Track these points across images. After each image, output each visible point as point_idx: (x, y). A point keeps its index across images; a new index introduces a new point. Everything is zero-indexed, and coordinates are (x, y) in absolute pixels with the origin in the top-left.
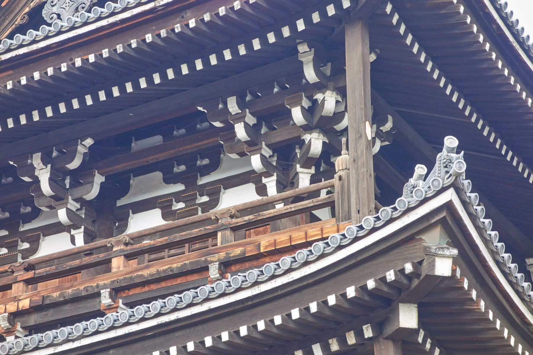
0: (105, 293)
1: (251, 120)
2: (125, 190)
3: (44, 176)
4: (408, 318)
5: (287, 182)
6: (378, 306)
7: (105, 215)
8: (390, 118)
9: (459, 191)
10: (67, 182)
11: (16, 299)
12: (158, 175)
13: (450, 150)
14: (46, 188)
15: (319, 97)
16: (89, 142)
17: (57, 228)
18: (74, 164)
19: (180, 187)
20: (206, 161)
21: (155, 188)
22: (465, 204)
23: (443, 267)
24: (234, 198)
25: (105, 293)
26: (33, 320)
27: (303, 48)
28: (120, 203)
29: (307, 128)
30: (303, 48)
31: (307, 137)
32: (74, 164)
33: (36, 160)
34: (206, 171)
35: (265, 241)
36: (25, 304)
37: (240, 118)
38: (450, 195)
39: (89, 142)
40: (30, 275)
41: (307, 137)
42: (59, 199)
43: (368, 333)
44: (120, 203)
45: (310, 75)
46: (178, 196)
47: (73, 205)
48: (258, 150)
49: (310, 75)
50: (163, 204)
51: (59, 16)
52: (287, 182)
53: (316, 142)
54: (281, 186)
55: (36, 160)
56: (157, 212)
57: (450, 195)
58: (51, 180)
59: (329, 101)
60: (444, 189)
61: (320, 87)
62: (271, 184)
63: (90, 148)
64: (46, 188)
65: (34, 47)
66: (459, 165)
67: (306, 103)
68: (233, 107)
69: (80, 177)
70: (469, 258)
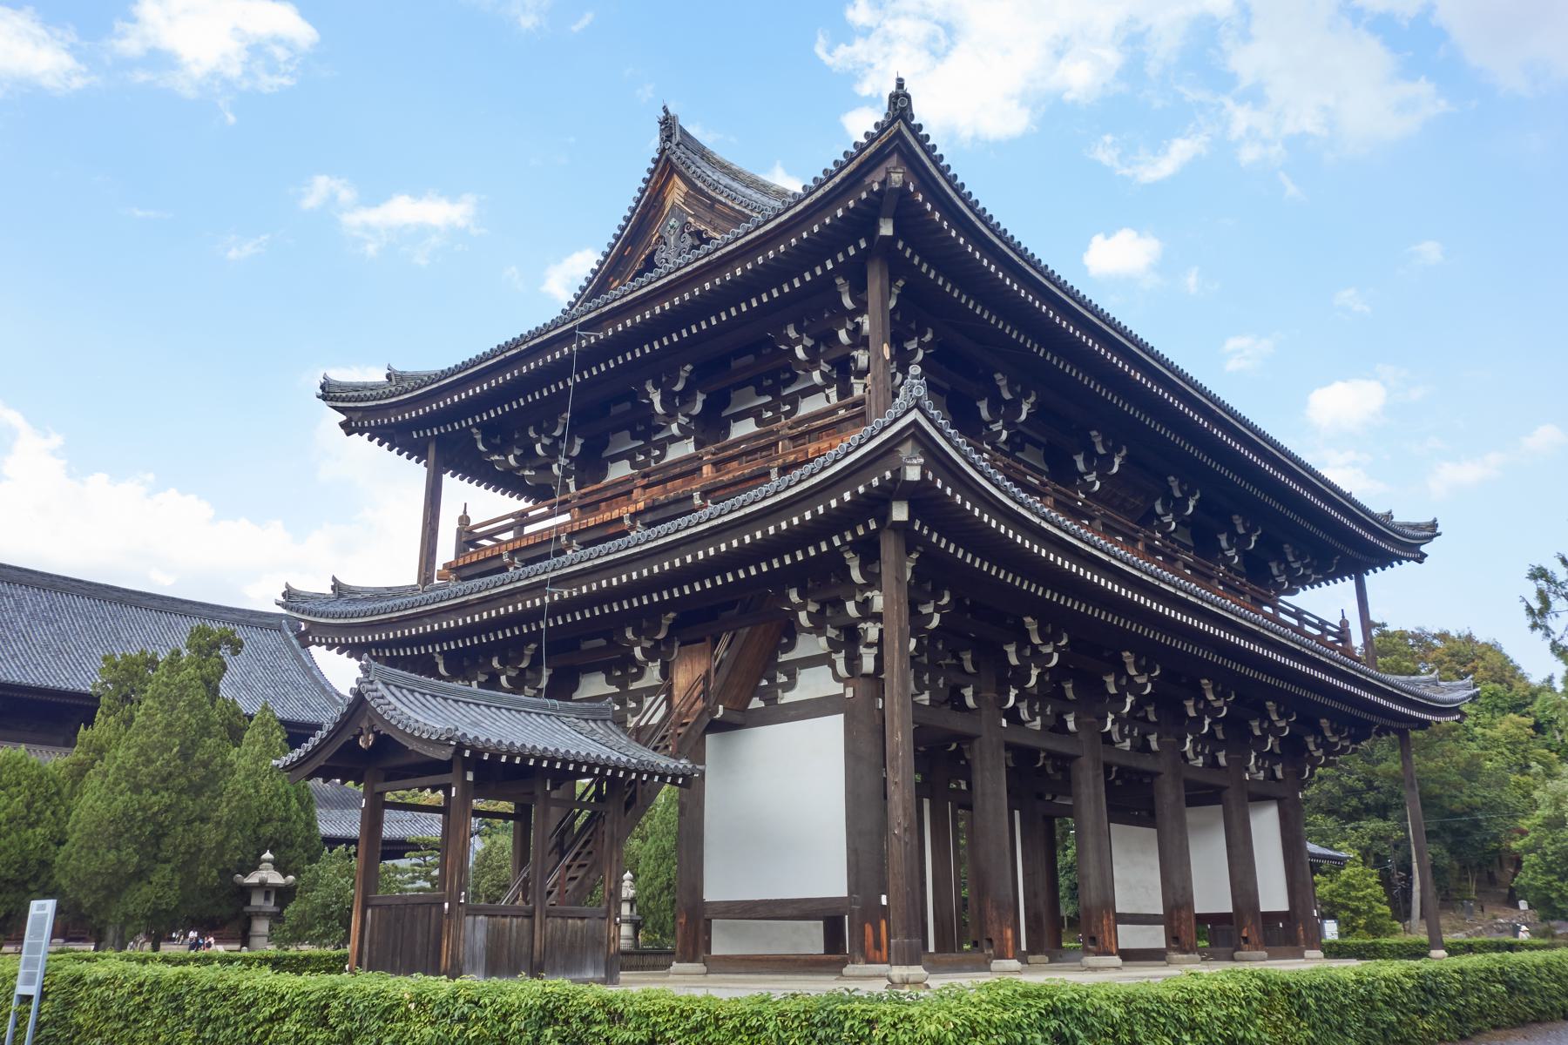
0: (696, 495)
1: (809, 342)
2: (726, 403)
3: (656, 398)
4: (900, 513)
7: (711, 426)
8: (930, 330)
9: (923, 411)
11: (636, 502)
13: (915, 377)
14: (658, 408)
15: (859, 319)
16: (689, 367)
17: (673, 439)
18: (679, 387)
21: (752, 400)
22: (931, 421)
23: (913, 474)
25: (696, 495)
26: (649, 518)
27: (839, 281)
28: (724, 414)
29: (854, 346)
30: (839, 281)
31: (855, 353)
32: (679, 387)
33: (649, 388)
34: (788, 383)
36: (641, 505)
37: (799, 341)
38: (915, 415)
39: (689, 367)
40: (645, 481)
41: (855, 353)
42: (671, 416)
43: (873, 526)
44: (724, 414)
46: (767, 407)
47: (683, 420)
48: (817, 367)
50: (755, 413)
54: (841, 396)
55: (649, 388)
56: (752, 420)
57: (915, 415)
58: (663, 402)
60: (908, 411)
63: (691, 372)
64: (658, 408)
66: (920, 390)
68: (792, 334)
69: (687, 396)
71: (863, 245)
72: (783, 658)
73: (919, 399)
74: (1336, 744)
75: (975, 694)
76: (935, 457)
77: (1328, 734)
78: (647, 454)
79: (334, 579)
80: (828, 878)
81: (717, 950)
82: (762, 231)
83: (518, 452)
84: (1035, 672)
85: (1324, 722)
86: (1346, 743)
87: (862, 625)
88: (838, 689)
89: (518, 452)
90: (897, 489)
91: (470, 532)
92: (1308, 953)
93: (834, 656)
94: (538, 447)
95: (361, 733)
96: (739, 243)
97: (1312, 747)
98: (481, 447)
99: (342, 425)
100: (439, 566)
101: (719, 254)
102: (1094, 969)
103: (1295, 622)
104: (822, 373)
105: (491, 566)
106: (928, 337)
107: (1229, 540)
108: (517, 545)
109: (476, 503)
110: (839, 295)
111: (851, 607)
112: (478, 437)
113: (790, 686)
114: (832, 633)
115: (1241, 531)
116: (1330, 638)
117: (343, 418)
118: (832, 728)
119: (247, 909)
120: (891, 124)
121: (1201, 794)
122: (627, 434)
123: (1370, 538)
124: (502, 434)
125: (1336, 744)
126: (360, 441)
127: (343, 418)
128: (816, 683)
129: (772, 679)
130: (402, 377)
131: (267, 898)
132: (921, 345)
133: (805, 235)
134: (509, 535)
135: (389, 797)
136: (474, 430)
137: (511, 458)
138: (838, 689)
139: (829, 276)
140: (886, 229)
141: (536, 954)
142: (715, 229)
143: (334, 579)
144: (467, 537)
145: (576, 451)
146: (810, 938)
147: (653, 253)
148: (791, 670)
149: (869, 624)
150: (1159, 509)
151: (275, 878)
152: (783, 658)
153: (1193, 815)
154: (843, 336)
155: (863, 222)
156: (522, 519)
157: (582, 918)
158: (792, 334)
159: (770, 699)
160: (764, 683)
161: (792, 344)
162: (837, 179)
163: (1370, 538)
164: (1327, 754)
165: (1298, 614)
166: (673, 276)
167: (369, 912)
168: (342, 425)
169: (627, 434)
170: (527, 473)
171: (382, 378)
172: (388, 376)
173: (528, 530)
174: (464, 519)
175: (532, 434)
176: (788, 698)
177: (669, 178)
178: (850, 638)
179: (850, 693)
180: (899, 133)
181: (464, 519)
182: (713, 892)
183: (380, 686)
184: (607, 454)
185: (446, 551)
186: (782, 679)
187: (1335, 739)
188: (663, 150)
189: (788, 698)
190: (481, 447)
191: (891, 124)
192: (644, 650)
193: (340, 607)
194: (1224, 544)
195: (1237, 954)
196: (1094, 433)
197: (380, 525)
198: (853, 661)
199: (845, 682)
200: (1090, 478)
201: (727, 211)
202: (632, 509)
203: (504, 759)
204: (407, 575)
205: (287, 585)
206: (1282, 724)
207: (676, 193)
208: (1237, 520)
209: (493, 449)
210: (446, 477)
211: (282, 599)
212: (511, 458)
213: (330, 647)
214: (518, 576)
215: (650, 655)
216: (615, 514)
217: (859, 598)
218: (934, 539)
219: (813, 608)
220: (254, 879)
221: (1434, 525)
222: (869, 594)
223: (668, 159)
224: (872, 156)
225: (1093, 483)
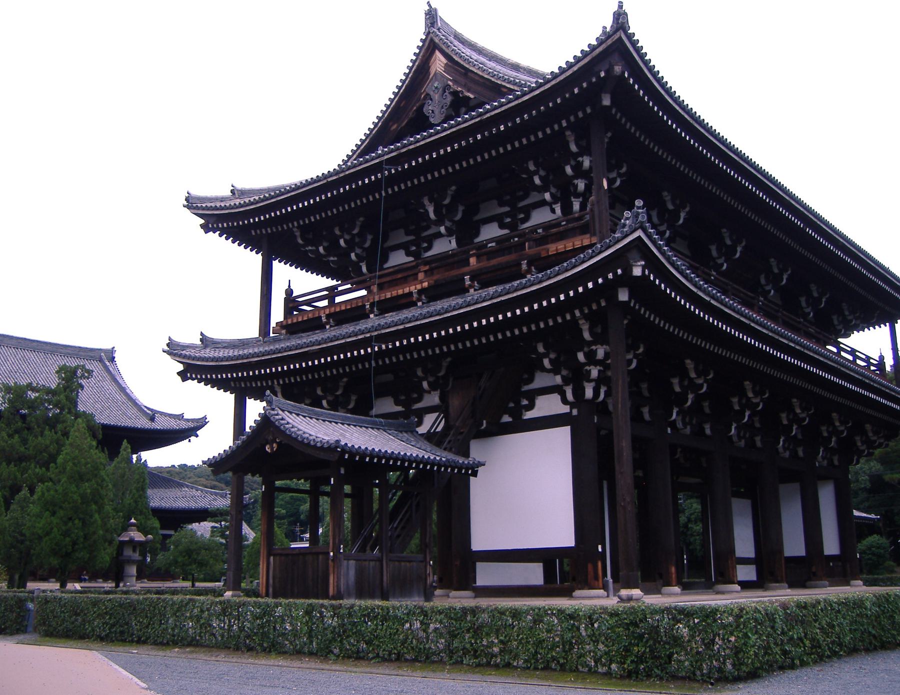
1: (542, 173)
2: (477, 211)
4: (623, 296)
5: (567, 209)
6: (609, 289)
8: (625, 165)
9: (645, 231)
10: (444, 211)
11: (421, 282)
12: (495, 202)
13: (639, 208)
14: (432, 216)
15: (580, 159)
18: (447, 202)
19: (507, 209)
20: (521, 193)
22: (649, 236)
23: (637, 272)
24: (540, 217)
27: (568, 133)
29: (576, 177)
30: (568, 133)
31: (576, 181)
32: (447, 202)
33: (426, 201)
35: (554, 248)
36: (425, 284)
37: (536, 173)
38: (639, 233)
39: (454, 188)
40: (427, 268)
41: (576, 181)
45: (574, 148)
46: (507, 214)
49: (574, 148)
51: (433, 111)
53: (581, 185)
55: (426, 201)
58: (435, 212)
59: (586, 163)
64: (432, 216)
65: (418, 145)
67: (573, 163)
68: (532, 167)
69: (452, 208)
70: (652, 263)
71: (589, 110)
72: (526, 388)
73: (642, 223)
74: (875, 441)
75: (650, 412)
76: (652, 263)
77: (870, 434)
78: (418, 246)
79: (202, 334)
80: (562, 534)
81: (480, 582)
82: (520, 101)
83: (326, 244)
84: (690, 396)
85: (868, 427)
86: (882, 441)
87: (587, 368)
88: (566, 409)
89: (326, 244)
90: (627, 280)
92: (853, 582)
93: (565, 388)
94: (342, 242)
95: (267, 443)
96: (503, 109)
97: (859, 444)
98: (300, 241)
99: (202, 226)
100: (273, 324)
101: (488, 115)
102: (723, 593)
103: (850, 358)
104: (551, 195)
105: (314, 324)
106: (624, 170)
107: (807, 301)
108: (333, 310)
109: (297, 280)
110: (567, 143)
111: (581, 357)
112: (298, 234)
113: (531, 407)
114: (564, 372)
115: (815, 294)
116: (872, 368)
117: (202, 221)
118: (562, 436)
119: (121, 558)
120: (615, 32)
121: (787, 476)
122: (402, 231)
124: (313, 233)
125: (875, 441)
126: (214, 236)
127: (202, 221)
128: (549, 405)
129: (518, 403)
130: (243, 193)
131: (134, 551)
132: (620, 175)
133: (551, 105)
134: (325, 303)
135: (278, 483)
136: (295, 230)
137: (321, 249)
138: (566, 409)
139: (562, 130)
140: (606, 101)
141: (385, 584)
142: (468, 91)
143: (202, 334)
146: (534, 574)
148: (532, 396)
149: (592, 367)
150: (763, 281)
151: (138, 537)
152: (526, 388)
153: (783, 489)
154: (569, 170)
155: (591, 96)
156: (332, 292)
157: (410, 562)
158: (532, 167)
159: (517, 413)
160: (512, 405)
161: (531, 174)
162: (575, 68)
164: (868, 448)
165: (853, 352)
166: (454, 130)
167: (272, 558)
168: (202, 226)
169: (402, 231)
170: (332, 259)
171: (228, 193)
172: (232, 191)
173: (338, 299)
174: (289, 292)
175: (337, 232)
176: (529, 415)
177: (433, 53)
178: (577, 377)
179: (575, 412)
180: (620, 38)
181: (289, 292)
182: (479, 543)
183: (280, 412)
185: (277, 314)
186: (525, 402)
187: (875, 438)
188: (429, 33)
189: (529, 415)
190: (300, 241)
191: (615, 32)
192: (429, 383)
193: (209, 353)
195: (808, 583)
196: (724, 230)
197: (234, 295)
198: (579, 392)
199: (572, 405)
200: (720, 261)
201: (477, 78)
202: (419, 287)
203: (367, 460)
204: (253, 332)
205: (170, 339)
206: (842, 428)
207: (439, 63)
208: (813, 287)
209: (308, 242)
210: (275, 263)
211: (166, 348)
212: (321, 249)
214: (333, 334)
215: (433, 387)
216: (407, 290)
217: (586, 349)
218: (642, 312)
219: (552, 356)
220: (125, 538)
222: (594, 347)
223: (432, 40)
224: (600, 53)
225: (722, 265)
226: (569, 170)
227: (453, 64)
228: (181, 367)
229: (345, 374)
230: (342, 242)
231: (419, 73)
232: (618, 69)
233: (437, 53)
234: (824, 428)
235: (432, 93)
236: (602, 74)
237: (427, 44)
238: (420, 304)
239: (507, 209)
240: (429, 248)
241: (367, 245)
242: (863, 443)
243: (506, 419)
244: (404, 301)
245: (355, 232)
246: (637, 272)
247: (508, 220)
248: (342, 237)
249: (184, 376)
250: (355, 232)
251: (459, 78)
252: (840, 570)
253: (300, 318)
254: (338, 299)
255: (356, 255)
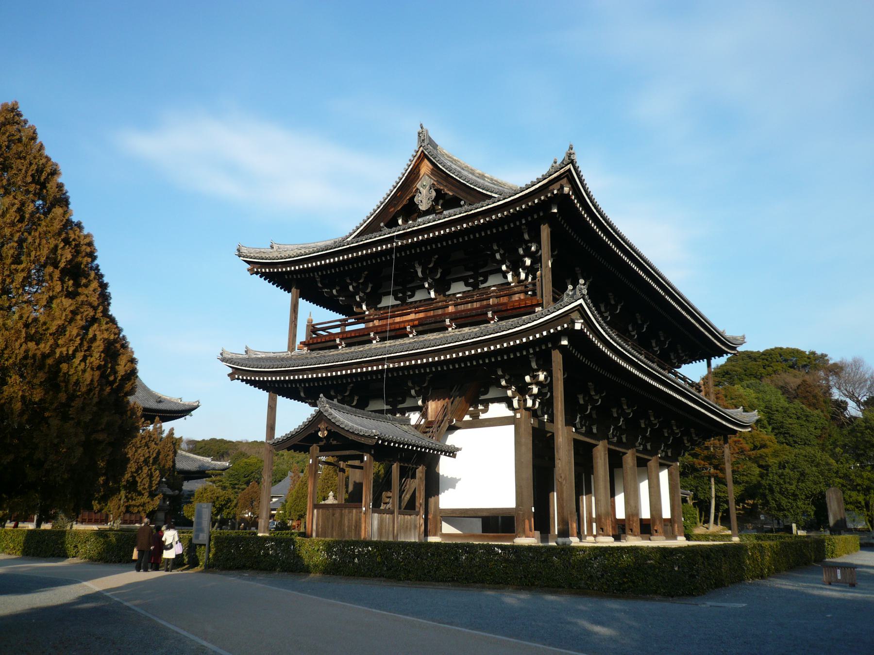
1: (502, 252)
5: (517, 274)
14: (420, 274)
18: (431, 266)
19: (471, 273)
23: (578, 326)
28: (448, 278)
32: (431, 266)
34: (483, 267)
37: (498, 251)
38: (581, 301)
42: (424, 279)
43: (550, 346)
44: (448, 278)
45: (526, 237)
49: (526, 237)
52: (517, 274)
53: (528, 262)
57: (581, 301)
61: (531, 241)
62: (510, 277)
64: (420, 274)
70: (588, 322)
71: (541, 214)
76: (588, 322)
77: (694, 436)
85: (692, 430)
88: (511, 413)
91: (313, 326)
94: (351, 288)
95: (320, 430)
98: (320, 285)
100: (298, 343)
113: (485, 411)
123: (718, 344)
127: (249, 266)
134: (338, 330)
137: (334, 292)
144: (313, 329)
145: (369, 290)
147: (414, 197)
150: (630, 328)
154: (521, 251)
155: (545, 205)
156: (344, 324)
158: (495, 248)
159: (475, 416)
163: (718, 344)
165: (684, 379)
174: (310, 322)
176: (483, 416)
177: (422, 160)
179: (518, 416)
180: (569, 170)
184: (380, 291)
185: (302, 336)
189: (483, 416)
190: (320, 285)
194: (654, 345)
208: (661, 333)
209: (325, 287)
212: (334, 292)
213: (243, 380)
221: (744, 337)
224: (555, 178)
226: (521, 251)
227: (437, 171)
228: (230, 371)
229: (352, 382)
230: (351, 288)
231: (412, 176)
232: (566, 190)
233: (426, 160)
234: (665, 431)
235: (421, 189)
236: (555, 192)
237: (419, 153)
238: (411, 336)
239: (471, 273)
240: (412, 296)
241: (369, 290)
242: (688, 441)
243: (467, 418)
244: (399, 332)
245: (361, 281)
246: (578, 326)
247: (471, 281)
248: (351, 284)
249: (232, 376)
250: (361, 281)
251: (440, 180)
252: (669, 528)
253: (318, 340)
254: (348, 328)
255: (360, 297)
